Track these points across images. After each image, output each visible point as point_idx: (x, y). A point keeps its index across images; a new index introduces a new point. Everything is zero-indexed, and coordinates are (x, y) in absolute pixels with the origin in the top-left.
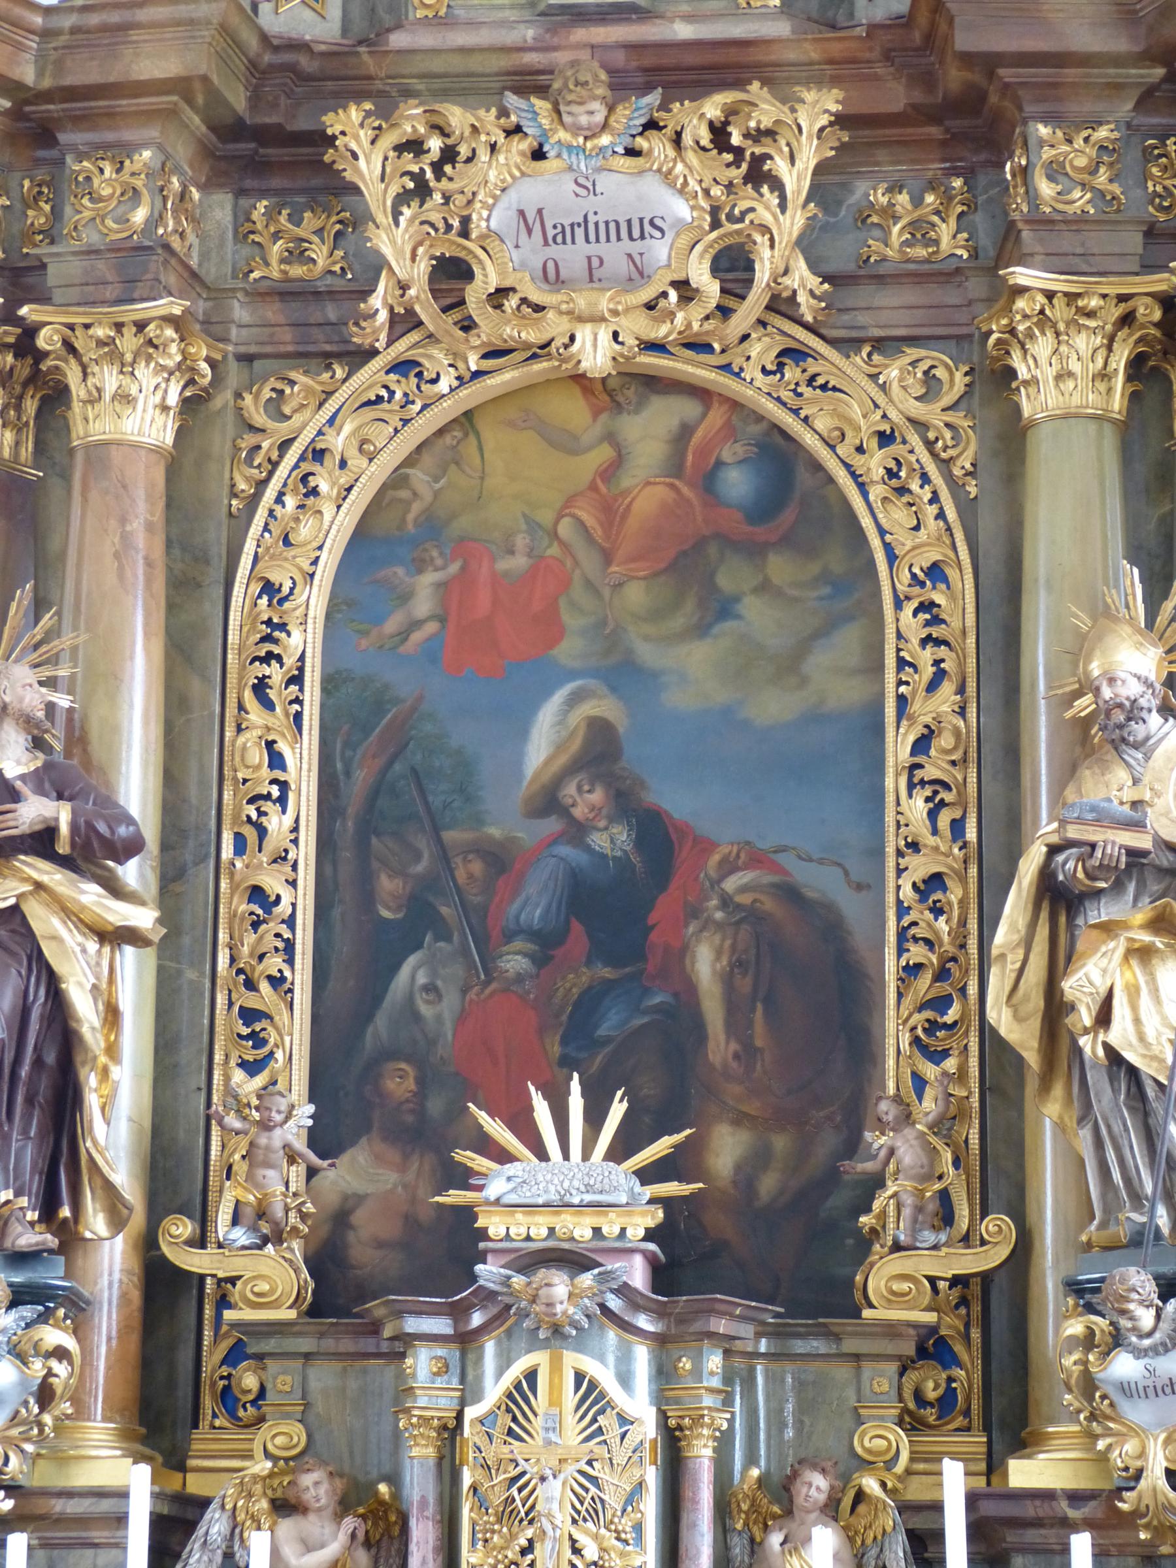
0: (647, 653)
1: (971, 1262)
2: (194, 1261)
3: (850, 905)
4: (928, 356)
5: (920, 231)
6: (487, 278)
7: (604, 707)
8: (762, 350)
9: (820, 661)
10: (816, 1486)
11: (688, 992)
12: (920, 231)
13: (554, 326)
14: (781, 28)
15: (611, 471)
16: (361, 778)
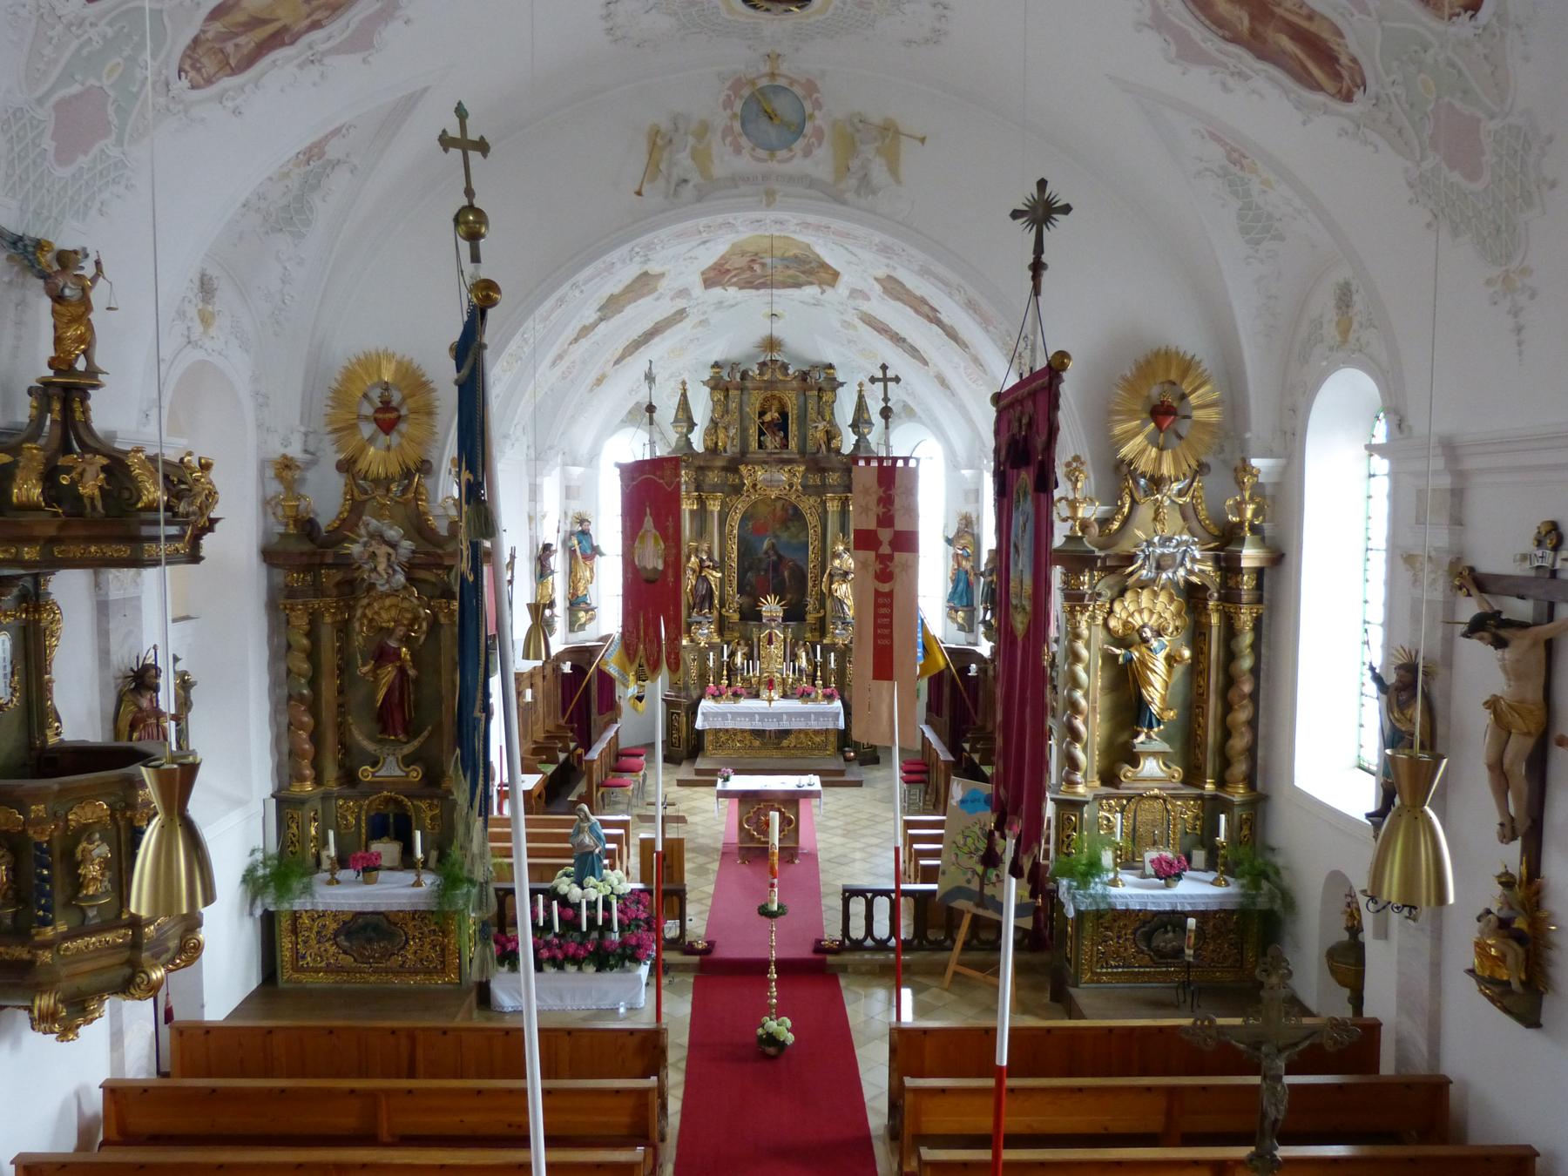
0: (778, 533)
1: (819, 615)
2: (726, 614)
3: (805, 567)
4: (815, 498)
5: (814, 480)
6: (758, 487)
7: (773, 541)
8: (793, 497)
9: (801, 535)
10: (801, 642)
11: (784, 579)
12: (814, 480)
13: (768, 492)
14: (798, 456)
15: (774, 510)
16: (742, 550)
